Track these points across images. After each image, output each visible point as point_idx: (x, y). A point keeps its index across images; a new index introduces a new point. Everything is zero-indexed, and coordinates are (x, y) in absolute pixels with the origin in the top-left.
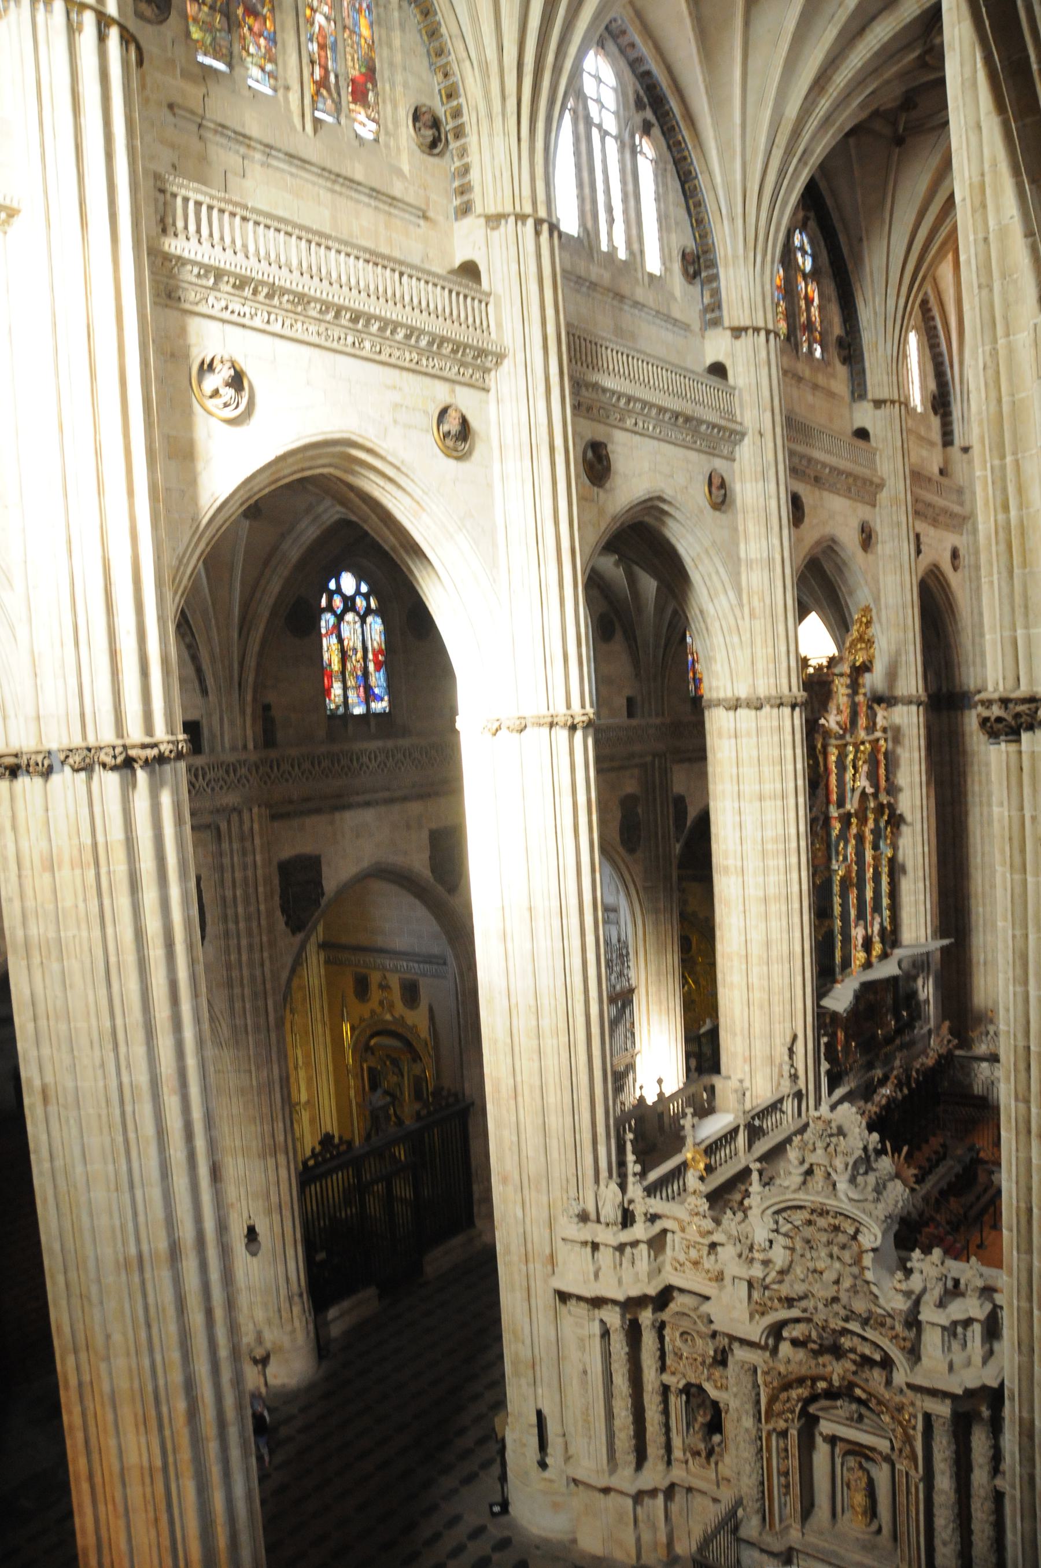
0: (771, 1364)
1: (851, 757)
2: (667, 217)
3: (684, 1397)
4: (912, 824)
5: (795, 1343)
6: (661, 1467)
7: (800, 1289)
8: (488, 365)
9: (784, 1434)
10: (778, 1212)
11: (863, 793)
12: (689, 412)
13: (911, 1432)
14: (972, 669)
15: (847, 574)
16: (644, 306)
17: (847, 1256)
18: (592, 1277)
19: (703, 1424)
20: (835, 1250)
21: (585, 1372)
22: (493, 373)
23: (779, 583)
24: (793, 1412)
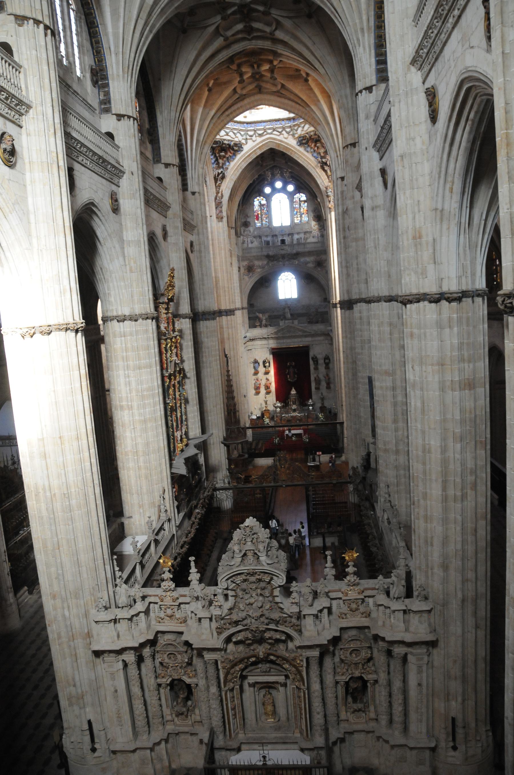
0: (225, 657)
1: (169, 345)
2: (83, 46)
3: (169, 688)
4: (189, 378)
5: (237, 643)
6: (161, 728)
7: (243, 615)
8: (22, 111)
9: (232, 690)
10: (227, 580)
11: (175, 363)
12: (104, 157)
13: (301, 668)
14: (200, 302)
15: (157, 252)
16: (78, 94)
17: (267, 593)
18: (116, 638)
19: (183, 698)
20: (259, 591)
21: (116, 691)
22: (24, 117)
23: (143, 254)
24: (236, 677)
